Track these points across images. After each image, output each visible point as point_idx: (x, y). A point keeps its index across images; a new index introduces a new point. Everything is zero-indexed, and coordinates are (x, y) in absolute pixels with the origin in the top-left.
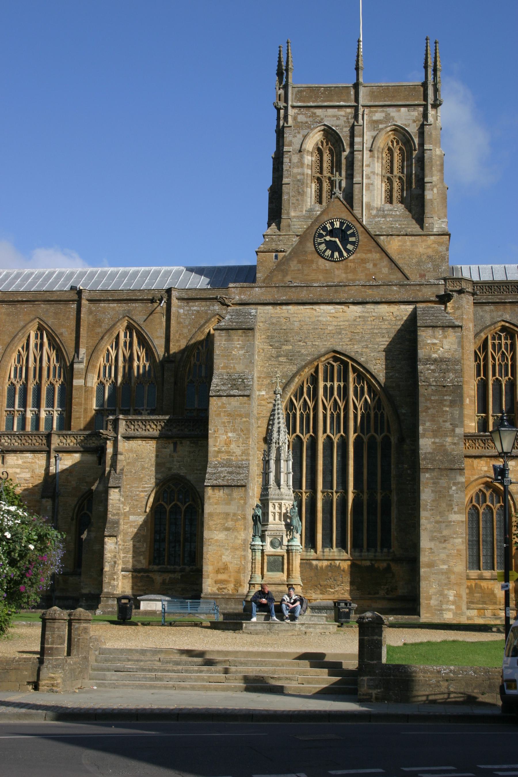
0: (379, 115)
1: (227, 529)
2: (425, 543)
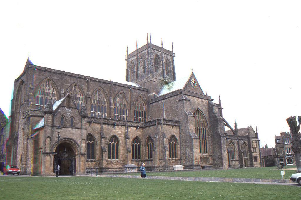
0: (165, 56)
1: (196, 149)
2: (223, 152)
